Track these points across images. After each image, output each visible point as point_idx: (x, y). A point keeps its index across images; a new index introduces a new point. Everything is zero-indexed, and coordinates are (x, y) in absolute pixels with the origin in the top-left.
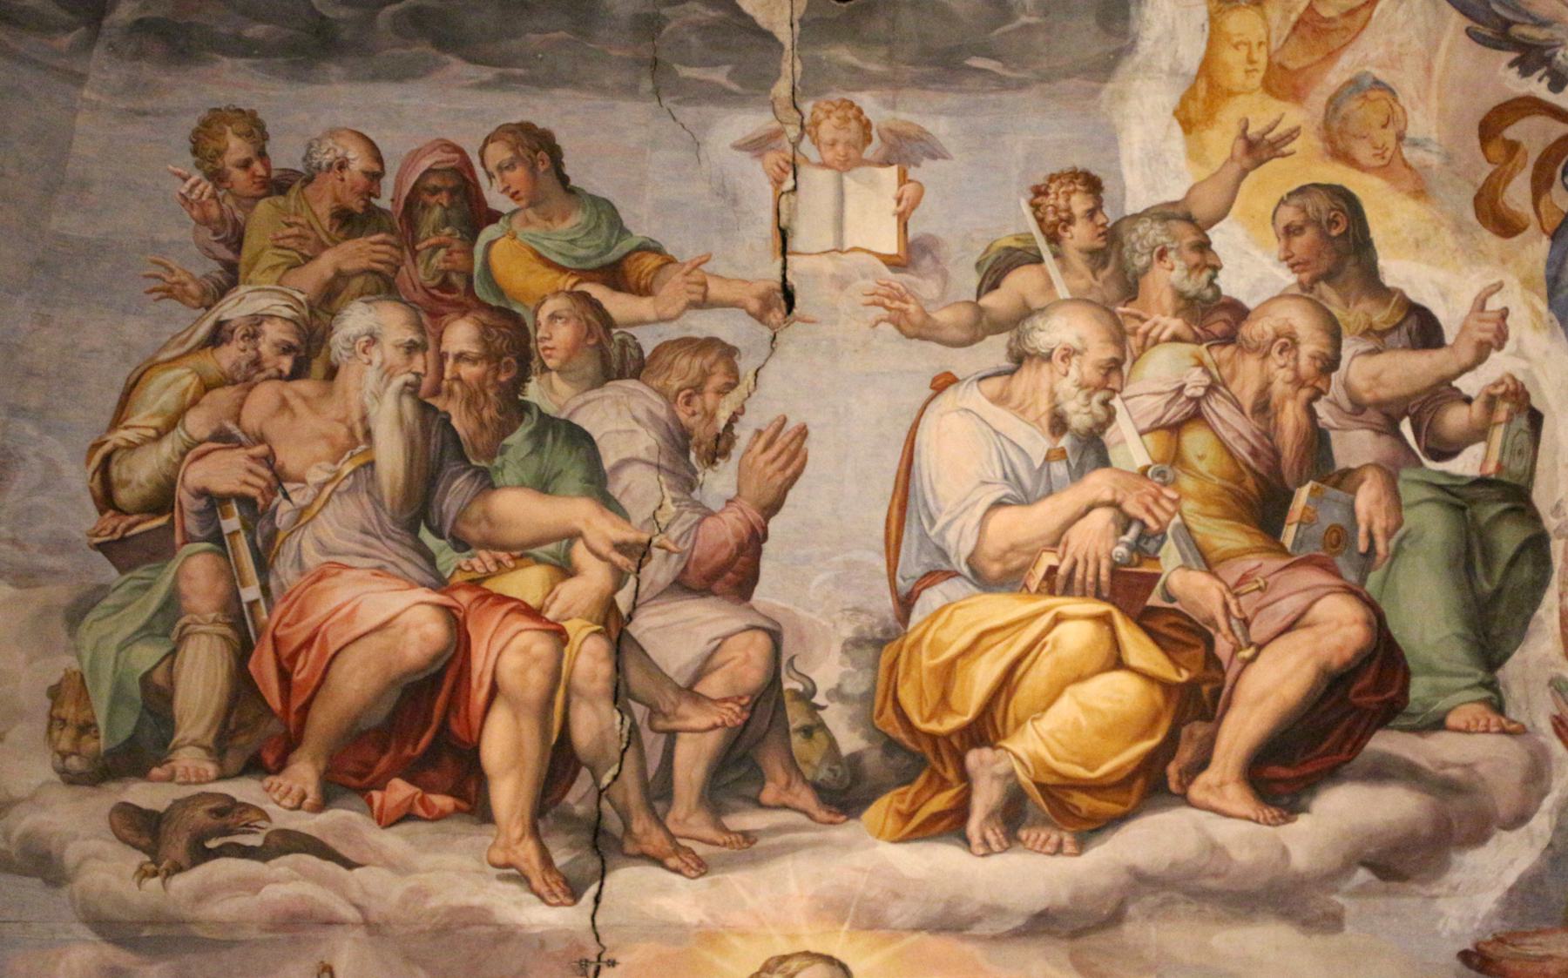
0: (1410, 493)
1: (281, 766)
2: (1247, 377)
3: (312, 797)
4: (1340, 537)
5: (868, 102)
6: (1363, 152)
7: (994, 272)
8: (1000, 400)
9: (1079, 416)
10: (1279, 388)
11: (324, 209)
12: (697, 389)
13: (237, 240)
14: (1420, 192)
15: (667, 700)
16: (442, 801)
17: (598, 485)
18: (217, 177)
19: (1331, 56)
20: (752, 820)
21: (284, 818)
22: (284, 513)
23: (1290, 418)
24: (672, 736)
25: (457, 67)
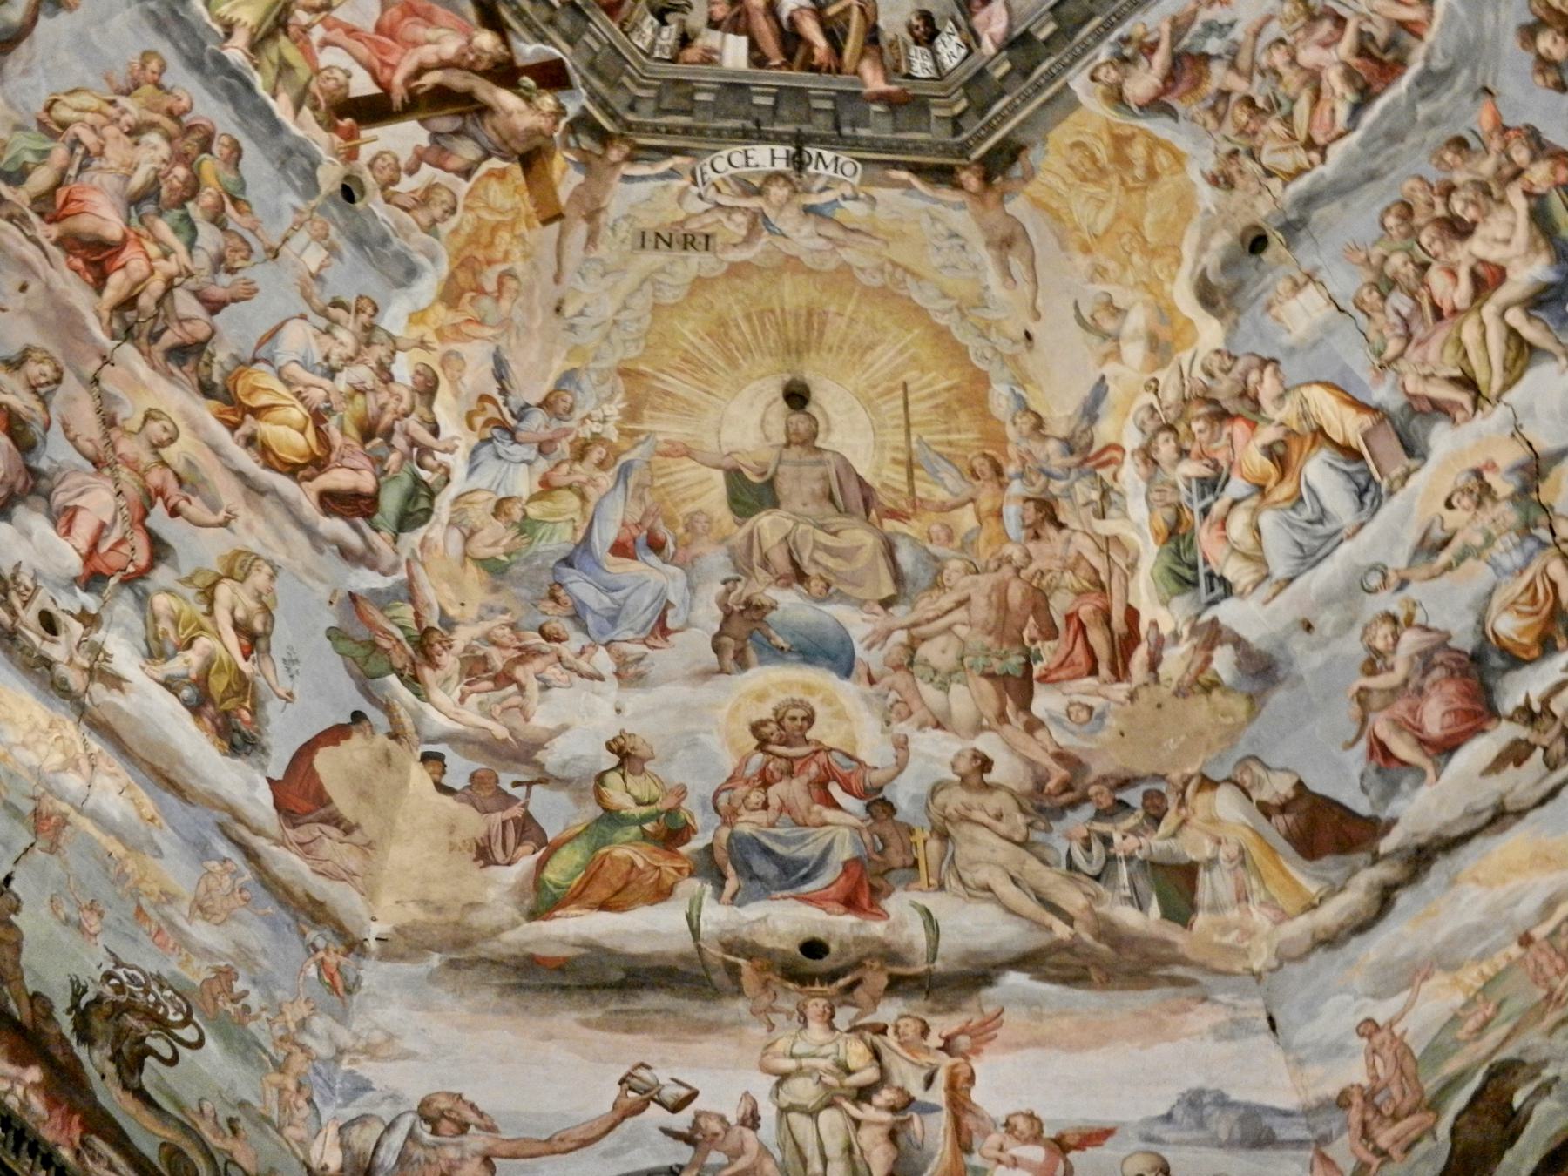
0: (406, 468)
1: (50, 222)
2: (384, 397)
3: (53, 238)
5: (333, 231)
6: (449, 371)
8: (316, 336)
9: (334, 361)
10: (391, 407)
11: (167, 102)
12: (236, 251)
13: (137, 86)
14: (456, 395)
15: (172, 317)
16: (89, 278)
17: (191, 245)
18: (143, 67)
19: (456, 340)
20: (175, 370)
22: (96, 163)
23: (387, 419)
24: (166, 328)
25: (230, 108)
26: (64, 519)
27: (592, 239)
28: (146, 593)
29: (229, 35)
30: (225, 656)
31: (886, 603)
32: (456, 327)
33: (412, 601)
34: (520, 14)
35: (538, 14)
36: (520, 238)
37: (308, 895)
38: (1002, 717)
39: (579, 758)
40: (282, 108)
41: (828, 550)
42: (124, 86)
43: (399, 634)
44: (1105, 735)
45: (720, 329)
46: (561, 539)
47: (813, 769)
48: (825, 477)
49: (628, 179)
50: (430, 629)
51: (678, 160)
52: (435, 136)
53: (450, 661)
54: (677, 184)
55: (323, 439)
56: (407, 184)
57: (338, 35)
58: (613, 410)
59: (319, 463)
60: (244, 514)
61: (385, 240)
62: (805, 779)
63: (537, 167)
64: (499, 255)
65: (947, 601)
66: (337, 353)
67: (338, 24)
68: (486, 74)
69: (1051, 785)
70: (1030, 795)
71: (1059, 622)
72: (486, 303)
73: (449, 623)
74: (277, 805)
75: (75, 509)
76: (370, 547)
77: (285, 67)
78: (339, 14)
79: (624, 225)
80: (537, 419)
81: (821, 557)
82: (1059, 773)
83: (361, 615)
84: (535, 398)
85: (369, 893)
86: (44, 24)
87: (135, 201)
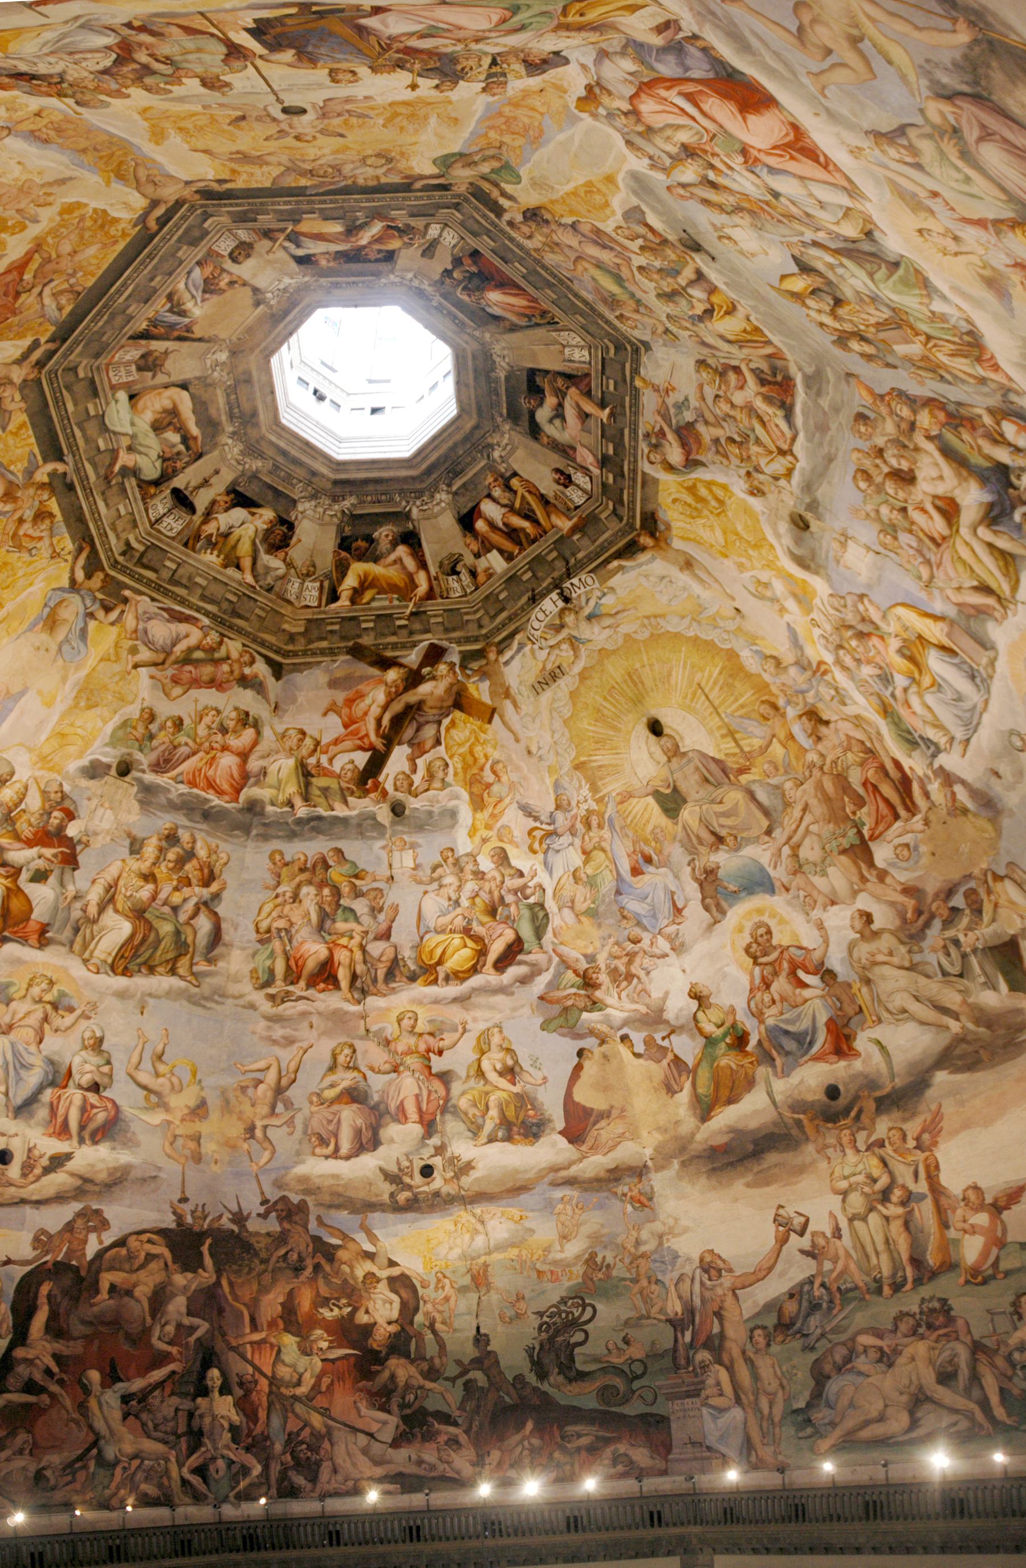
2: (487, 886)
4: (508, 917)
5: (406, 837)
7: (434, 870)
9: (454, 897)
17: (357, 920)
21: (299, 993)
23: (496, 894)
26: (401, 1116)
27: (515, 705)
28: (455, 1106)
29: (292, 807)
30: (504, 1095)
31: (769, 832)
32: (493, 816)
33: (568, 967)
34: (395, 646)
35: (402, 638)
36: (486, 742)
37: (610, 1171)
38: (863, 879)
39: (681, 1010)
40: (340, 811)
41: (726, 815)
42: (274, 883)
43: (573, 990)
44: (924, 861)
45: (599, 715)
46: (607, 883)
47: (785, 965)
48: (697, 769)
49: (506, 663)
50: (586, 971)
51: (518, 637)
52: (410, 743)
53: (603, 978)
54: (527, 649)
55: (477, 939)
56: (417, 779)
57: (333, 750)
58: (585, 791)
59: (482, 953)
60: (468, 1017)
61: (430, 813)
62: (784, 974)
63: (464, 701)
64: (482, 760)
65: (797, 813)
66: (451, 891)
67: (328, 745)
68: (406, 689)
69: (909, 915)
70: (901, 929)
71: (861, 791)
72: (495, 788)
73: (591, 958)
74: (570, 1142)
75: (402, 1103)
76: (532, 965)
77: (325, 791)
78: (324, 742)
79: (523, 689)
80: (560, 816)
81: (723, 821)
82: (910, 903)
83: (550, 1002)
84: (552, 807)
85: (635, 1137)
86: (220, 910)
87: (321, 928)
